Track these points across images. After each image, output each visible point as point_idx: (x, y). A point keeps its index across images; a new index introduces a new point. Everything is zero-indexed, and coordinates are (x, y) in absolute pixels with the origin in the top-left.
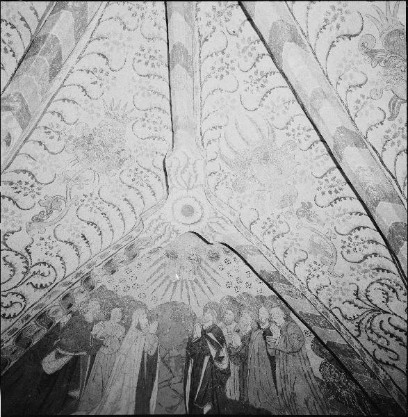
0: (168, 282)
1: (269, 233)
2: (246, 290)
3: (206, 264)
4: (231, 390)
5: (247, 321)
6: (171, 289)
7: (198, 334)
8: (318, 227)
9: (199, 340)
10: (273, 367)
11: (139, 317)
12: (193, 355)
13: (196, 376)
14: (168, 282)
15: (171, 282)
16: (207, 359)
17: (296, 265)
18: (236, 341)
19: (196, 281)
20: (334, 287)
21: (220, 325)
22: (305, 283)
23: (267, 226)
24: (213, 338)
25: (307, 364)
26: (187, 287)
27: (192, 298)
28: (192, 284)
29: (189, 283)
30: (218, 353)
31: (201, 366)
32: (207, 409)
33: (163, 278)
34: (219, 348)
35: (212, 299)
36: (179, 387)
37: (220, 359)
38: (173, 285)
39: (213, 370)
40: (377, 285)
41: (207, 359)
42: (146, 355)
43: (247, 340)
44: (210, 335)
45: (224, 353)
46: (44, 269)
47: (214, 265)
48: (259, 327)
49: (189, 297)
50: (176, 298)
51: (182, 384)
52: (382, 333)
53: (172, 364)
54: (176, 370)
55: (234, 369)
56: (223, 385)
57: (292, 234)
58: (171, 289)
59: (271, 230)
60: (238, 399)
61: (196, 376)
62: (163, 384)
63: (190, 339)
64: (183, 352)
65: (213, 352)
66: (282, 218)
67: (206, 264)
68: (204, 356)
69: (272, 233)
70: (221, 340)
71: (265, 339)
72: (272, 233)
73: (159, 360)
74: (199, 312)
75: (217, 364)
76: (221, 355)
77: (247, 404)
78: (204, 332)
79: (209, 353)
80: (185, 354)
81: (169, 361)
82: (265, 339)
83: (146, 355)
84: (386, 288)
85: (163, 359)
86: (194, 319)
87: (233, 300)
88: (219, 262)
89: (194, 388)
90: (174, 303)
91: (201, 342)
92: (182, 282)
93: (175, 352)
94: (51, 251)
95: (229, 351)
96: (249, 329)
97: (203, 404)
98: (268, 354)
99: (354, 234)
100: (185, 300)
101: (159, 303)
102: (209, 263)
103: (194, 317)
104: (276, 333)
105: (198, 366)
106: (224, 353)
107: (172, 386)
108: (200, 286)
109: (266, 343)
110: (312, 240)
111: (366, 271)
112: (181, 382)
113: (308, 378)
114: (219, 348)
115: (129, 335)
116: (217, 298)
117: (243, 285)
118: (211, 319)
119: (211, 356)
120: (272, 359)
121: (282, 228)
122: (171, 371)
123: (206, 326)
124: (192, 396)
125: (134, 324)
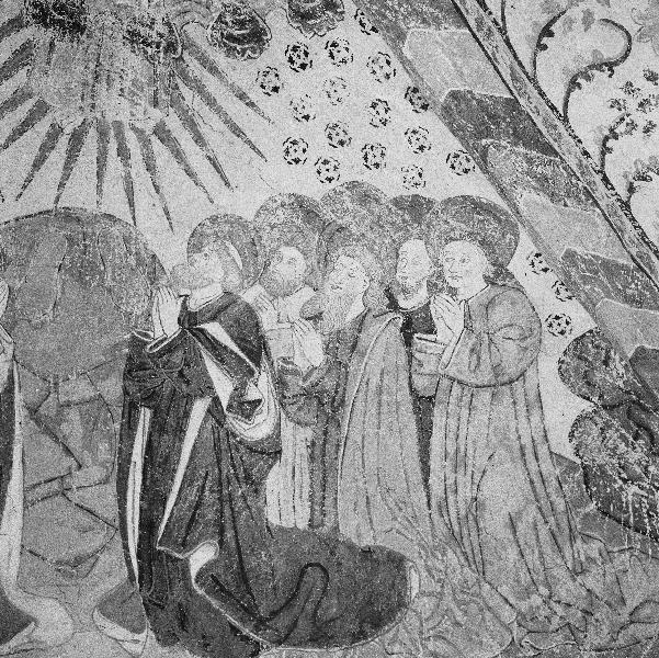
0: (42, 127)
3: (204, 61)
4: (283, 500)
5: (351, 282)
6: (57, 157)
7: (166, 324)
9: (170, 349)
10: (425, 431)
12: (150, 398)
13: (158, 464)
15: (55, 133)
16: (199, 408)
17: (573, 84)
18: (307, 351)
19: (162, 132)
21: (249, 296)
22: (594, 150)
24: (224, 338)
25: (535, 418)
26: (123, 153)
27: (144, 198)
28: (146, 143)
29: (130, 136)
30: (239, 391)
31: (180, 431)
32: (201, 556)
33: (22, 112)
35: (227, 202)
37: (247, 409)
38: (63, 143)
39: (221, 442)
41: (199, 408)
43: (344, 347)
44: (215, 330)
45: (261, 387)
47: (242, 72)
48: (394, 305)
49: (130, 192)
50: (80, 195)
51: (112, 488)
53: (73, 427)
54: (89, 445)
55: (296, 441)
56: (255, 485)
58: (57, 157)
60: (303, 525)
61: (158, 464)
62: (42, 490)
63: (137, 344)
64: (113, 388)
65: (224, 387)
67: (204, 61)
68: (190, 399)
70: (254, 346)
71: (408, 342)
73: (20, 414)
74: (171, 252)
75: (236, 424)
76: (252, 394)
77: (331, 543)
78: (189, 320)
79: (208, 388)
80: (119, 391)
81: (60, 418)
82: (408, 342)
85: (33, 411)
86: (153, 279)
87: (304, 208)
88: (263, 61)
89: (153, 498)
90: (68, 216)
91: (177, 357)
92: (103, 134)
93: (81, 389)
95: (280, 383)
96: (357, 308)
97: (186, 545)
98: (413, 391)
100: (115, 203)
102: (219, 57)
103: (153, 269)
104: (449, 318)
105: (168, 426)
106: (261, 387)
107: (75, 496)
108: (178, 155)
109: (410, 356)
112: (106, 481)
113: (530, 457)
116: (244, 204)
117: (349, 158)
118: (219, 275)
119: (216, 400)
120: (423, 405)
122: (68, 451)
124: (148, 525)
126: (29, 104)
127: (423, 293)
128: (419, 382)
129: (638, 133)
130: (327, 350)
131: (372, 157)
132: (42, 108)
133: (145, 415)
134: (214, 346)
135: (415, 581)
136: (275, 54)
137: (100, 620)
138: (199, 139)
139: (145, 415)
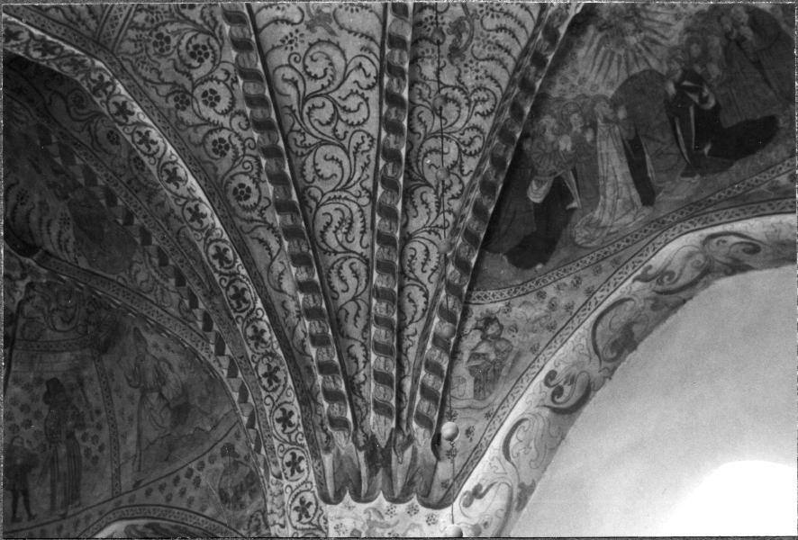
0: (616, 58)
7: (671, 88)
11: (603, 109)
14: (616, 58)
31: (689, 119)
34: (698, 91)
36: (674, 150)
37: (704, 100)
42: (626, 142)
44: (686, 83)
45: (706, 92)
46: (482, 95)
48: (730, 40)
51: (675, 145)
63: (666, 101)
64: (664, 117)
65: (695, 98)
68: (688, 110)
71: (741, 49)
74: (664, 70)
76: (705, 94)
78: (677, 85)
79: (691, 100)
82: (741, 49)
83: (626, 142)
89: (688, 142)
94: (479, 74)
101: (617, 86)
115: (600, 132)
119: (695, 103)
120: (758, 64)
123: (677, 76)
125: (600, 122)
126: (609, 55)
128: (751, 58)
130: (719, 67)
132: (613, 53)
135: (781, 121)
137: (682, 179)
138: (656, 32)
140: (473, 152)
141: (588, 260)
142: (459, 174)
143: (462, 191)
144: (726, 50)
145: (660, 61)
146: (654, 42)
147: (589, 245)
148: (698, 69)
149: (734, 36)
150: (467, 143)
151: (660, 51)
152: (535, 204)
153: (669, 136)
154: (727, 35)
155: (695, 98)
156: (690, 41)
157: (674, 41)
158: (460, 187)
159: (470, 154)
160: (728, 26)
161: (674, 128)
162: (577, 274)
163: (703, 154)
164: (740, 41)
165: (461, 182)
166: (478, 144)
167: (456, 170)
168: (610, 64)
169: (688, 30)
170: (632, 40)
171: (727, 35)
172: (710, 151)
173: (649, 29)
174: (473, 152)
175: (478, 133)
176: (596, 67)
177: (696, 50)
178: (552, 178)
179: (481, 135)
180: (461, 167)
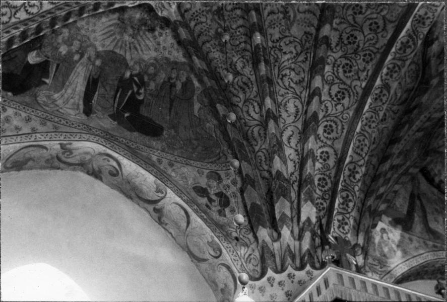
0: (114, 37)
1: (194, 20)
2: (167, 56)
7: (128, 74)
8: (222, 23)
11: (91, 52)
14: (114, 37)
20: (220, 60)
23: (195, 15)
34: (139, 87)
36: (111, 101)
37: (139, 94)
40: (242, 59)
42: (91, 77)
44: (136, 78)
45: (142, 91)
48: (169, 82)
51: (113, 100)
52: (237, 87)
54: (110, 91)
57: (207, 24)
59: (196, 18)
64: (116, 83)
65: (136, 89)
66: (205, 13)
68: (129, 90)
69: (196, 21)
71: (171, 88)
72: (196, 21)
74: (131, 64)
76: (141, 91)
78: (131, 76)
79: (133, 88)
82: (171, 88)
83: (91, 77)
84: (245, 61)
89: (119, 104)
98: (170, 98)
99: (238, 30)
101: (105, 49)
103: (127, 65)
109: (171, 91)
110: (217, 30)
111: (238, 51)
112: (112, 98)
114: (139, 87)
115: (82, 61)
120: (172, 101)
121: (203, 19)
123: (134, 72)
125: (86, 56)
127: (175, 80)
128: (172, 97)
129: (212, 53)
130: (155, 86)
131: (170, 53)
133: (121, 90)
134: (135, 81)
135: (165, 132)
136: (157, 33)
137: (108, 117)
138: (140, 45)
139: (121, 90)
140: (29, 11)
141: (40, 114)
142: (13, 13)
143: (7, 23)
144: (164, 82)
145: (132, 59)
146: (136, 48)
147: (44, 107)
148: (146, 78)
149: (172, 81)
150: (30, 4)
151: (135, 55)
152: (28, 62)
153: (113, 93)
154: (170, 78)
155: (136, 89)
156: (152, 64)
157: (146, 58)
158: (8, 20)
159: (27, 11)
160: (174, 76)
161: (117, 92)
162: (30, 116)
163: (124, 115)
164: (173, 86)
165: (10, 18)
166: (34, 10)
167: (13, 11)
168: (109, 37)
169: (156, 59)
170: (127, 38)
171: (170, 78)
172: (127, 117)
173: (138, 41)
174: (29, 11)
175: (39, 6)
176: (103, 32)
177: (151, 70)
178: (46, 58)
179: (39, 8)
180: (17, 11)
